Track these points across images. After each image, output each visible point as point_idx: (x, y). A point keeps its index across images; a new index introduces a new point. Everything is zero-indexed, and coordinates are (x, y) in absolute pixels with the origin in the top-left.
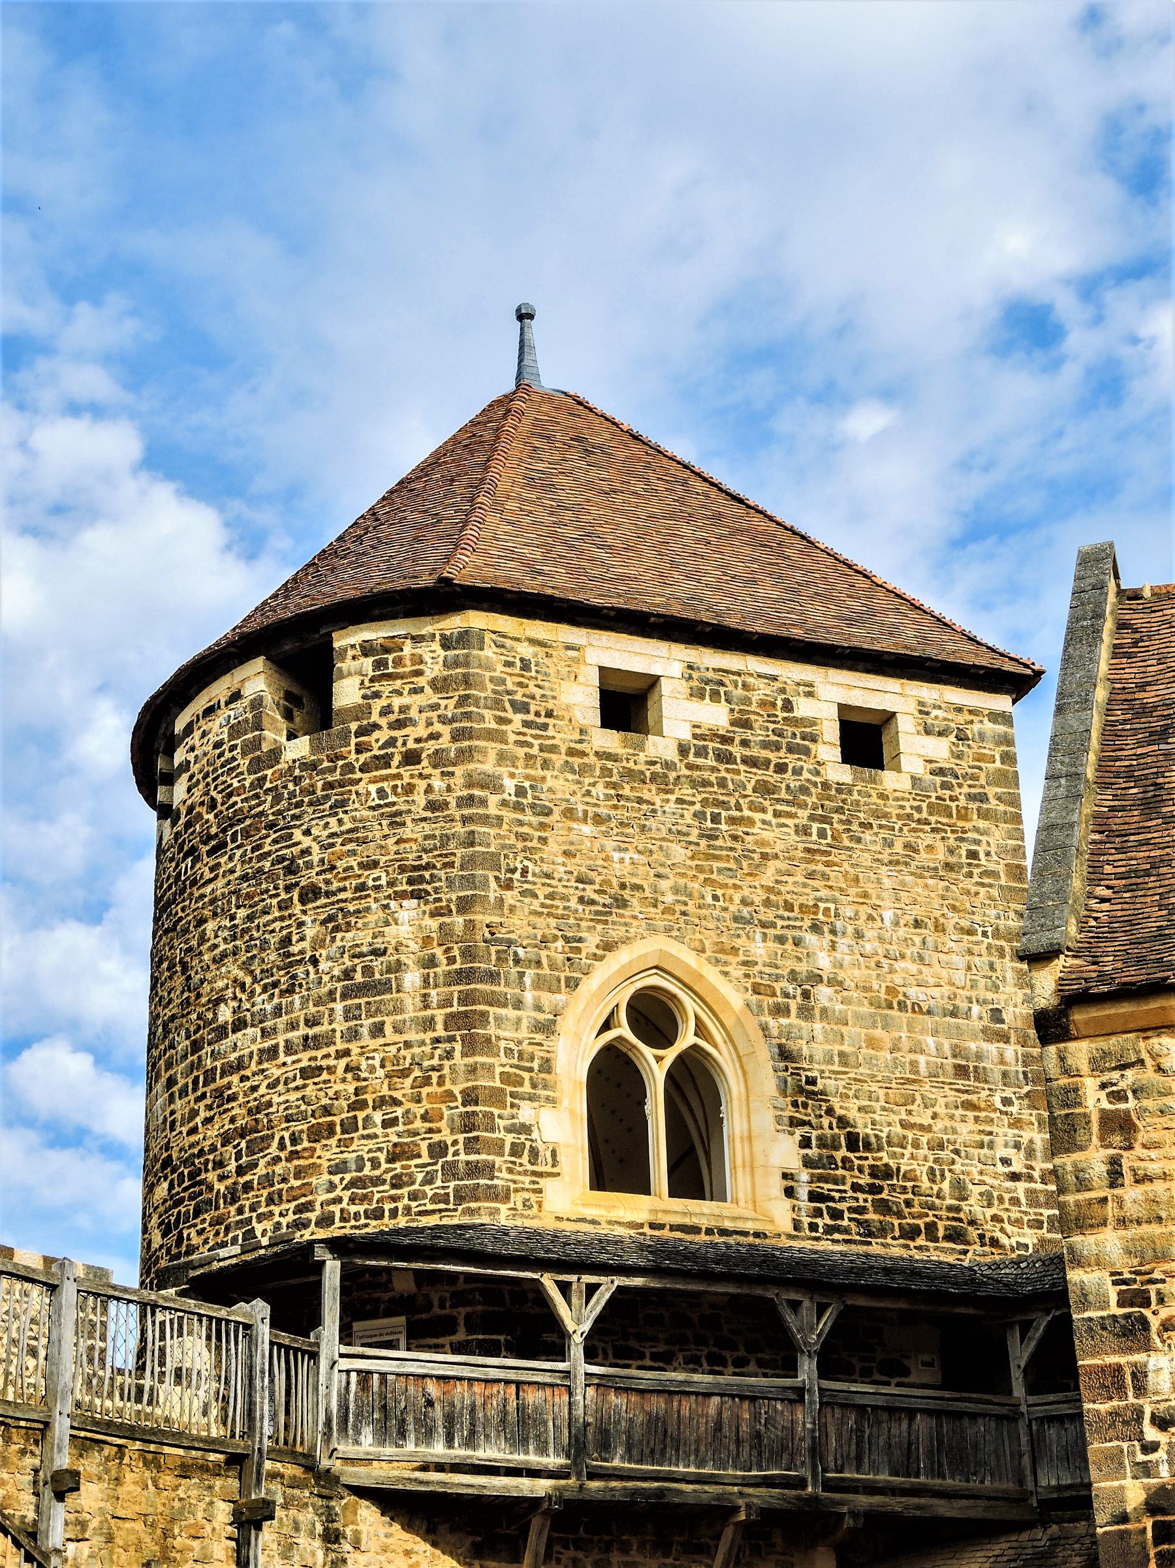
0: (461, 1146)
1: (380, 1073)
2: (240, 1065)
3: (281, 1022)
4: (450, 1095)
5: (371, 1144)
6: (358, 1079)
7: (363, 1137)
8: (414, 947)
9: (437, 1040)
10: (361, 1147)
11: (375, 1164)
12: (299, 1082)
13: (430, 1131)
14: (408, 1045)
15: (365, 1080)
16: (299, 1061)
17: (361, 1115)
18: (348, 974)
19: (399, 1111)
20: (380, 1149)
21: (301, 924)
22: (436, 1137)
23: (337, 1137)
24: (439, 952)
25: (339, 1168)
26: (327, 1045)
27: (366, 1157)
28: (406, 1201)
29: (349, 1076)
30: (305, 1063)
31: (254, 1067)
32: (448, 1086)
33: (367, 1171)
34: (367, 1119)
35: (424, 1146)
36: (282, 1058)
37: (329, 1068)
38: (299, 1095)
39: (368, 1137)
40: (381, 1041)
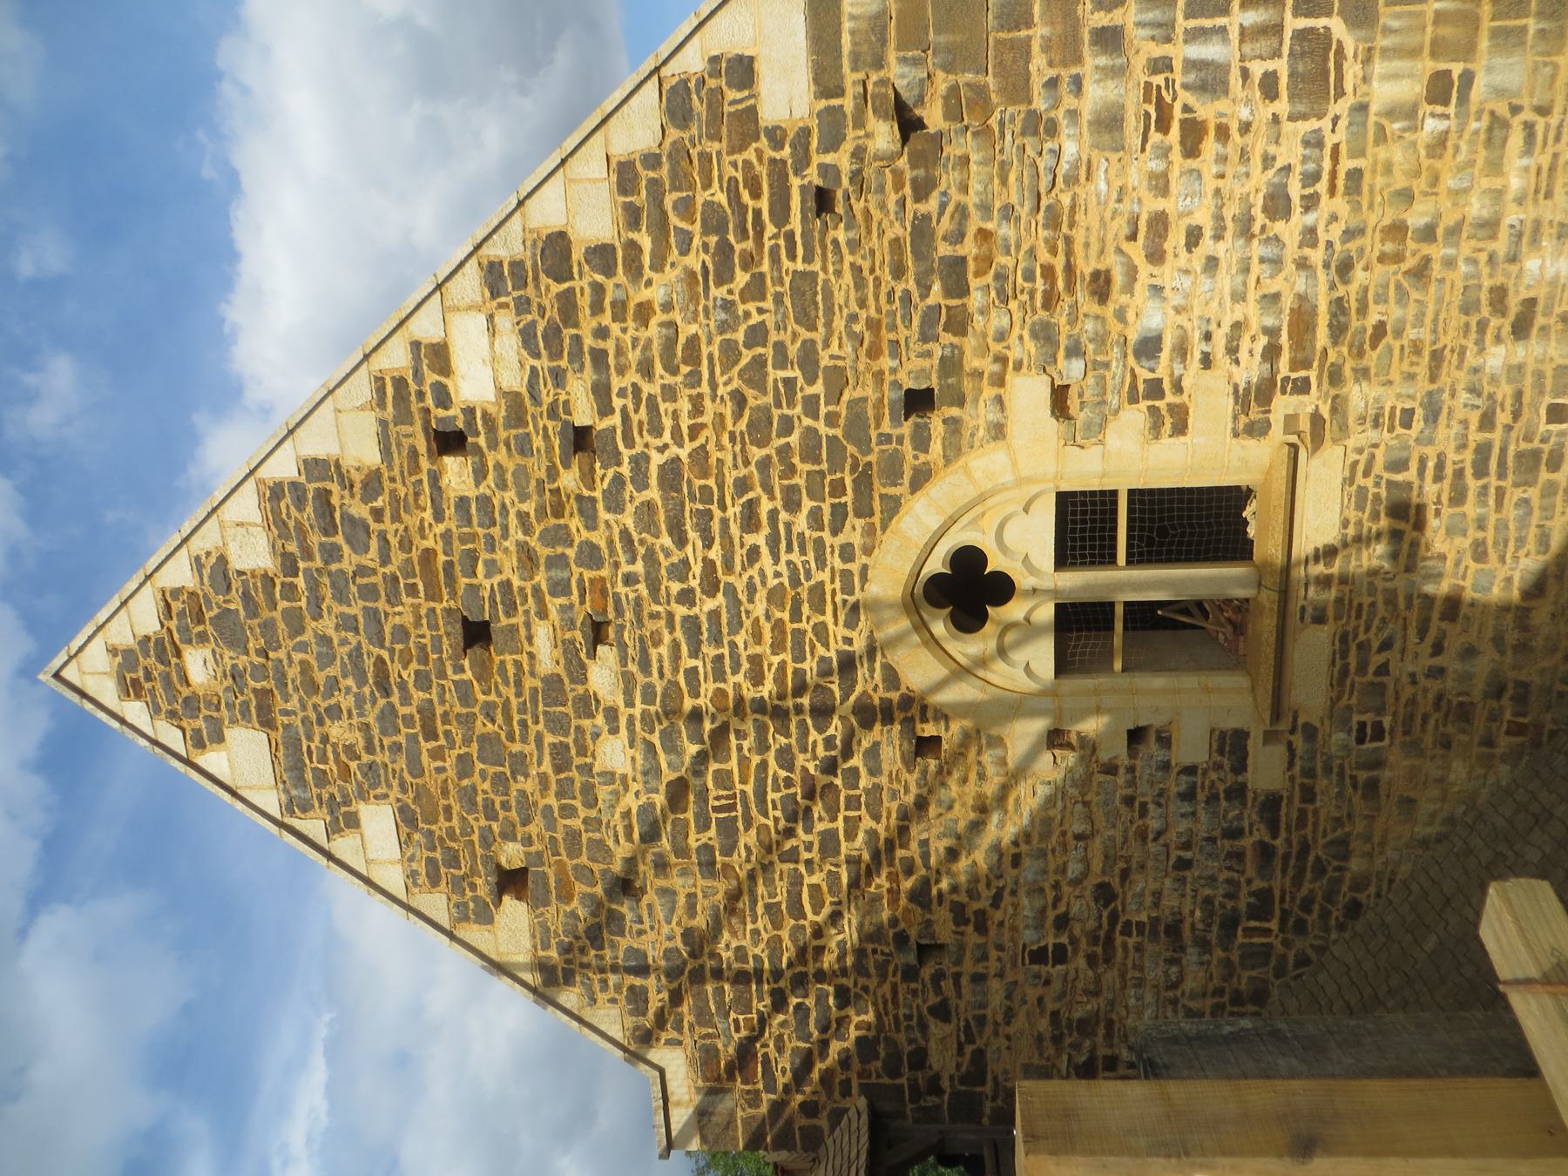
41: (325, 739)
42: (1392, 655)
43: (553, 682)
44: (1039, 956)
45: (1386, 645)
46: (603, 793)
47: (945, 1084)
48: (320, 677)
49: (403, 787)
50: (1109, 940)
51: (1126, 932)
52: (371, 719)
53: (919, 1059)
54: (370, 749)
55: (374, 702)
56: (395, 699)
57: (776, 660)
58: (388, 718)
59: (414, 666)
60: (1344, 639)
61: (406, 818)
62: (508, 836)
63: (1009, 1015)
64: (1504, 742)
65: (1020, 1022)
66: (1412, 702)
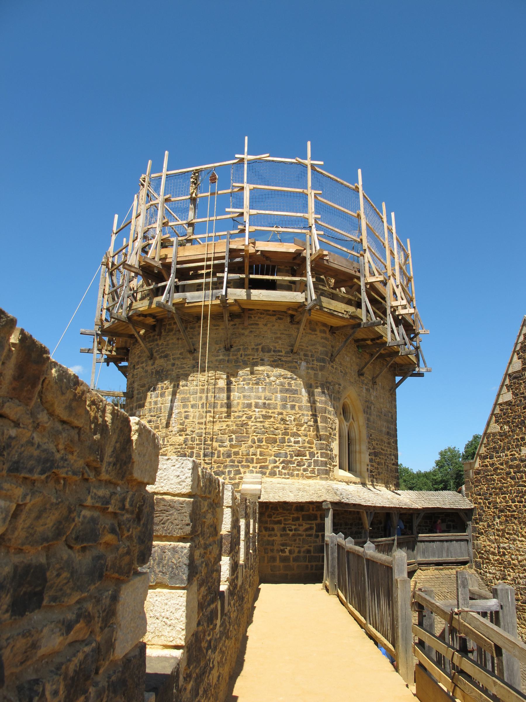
0: (319, 454)
3: (253, 394)
5: (290, 449)
7: (287, 446)
11: (292, 457)
12: (261, 420)
13: (310, 447)
14: (303, 415)
15: (288, 425)
16: (262, 411)
17: (287, 437)
18: (282, 384)
19: (300, 439)
22: (312, 450)
25: (277, 455)
26: (275, 408)
27: (288, 453)
28: (302, 472)
29: (282, 422)
30: (264, 413)
34: (289, 439)
36: (253, 408)
37: (274, 417)
39: (289, 446)
40: (294, 411)
53: (481, 520)
62: (510, 428)
65: (489, 543)
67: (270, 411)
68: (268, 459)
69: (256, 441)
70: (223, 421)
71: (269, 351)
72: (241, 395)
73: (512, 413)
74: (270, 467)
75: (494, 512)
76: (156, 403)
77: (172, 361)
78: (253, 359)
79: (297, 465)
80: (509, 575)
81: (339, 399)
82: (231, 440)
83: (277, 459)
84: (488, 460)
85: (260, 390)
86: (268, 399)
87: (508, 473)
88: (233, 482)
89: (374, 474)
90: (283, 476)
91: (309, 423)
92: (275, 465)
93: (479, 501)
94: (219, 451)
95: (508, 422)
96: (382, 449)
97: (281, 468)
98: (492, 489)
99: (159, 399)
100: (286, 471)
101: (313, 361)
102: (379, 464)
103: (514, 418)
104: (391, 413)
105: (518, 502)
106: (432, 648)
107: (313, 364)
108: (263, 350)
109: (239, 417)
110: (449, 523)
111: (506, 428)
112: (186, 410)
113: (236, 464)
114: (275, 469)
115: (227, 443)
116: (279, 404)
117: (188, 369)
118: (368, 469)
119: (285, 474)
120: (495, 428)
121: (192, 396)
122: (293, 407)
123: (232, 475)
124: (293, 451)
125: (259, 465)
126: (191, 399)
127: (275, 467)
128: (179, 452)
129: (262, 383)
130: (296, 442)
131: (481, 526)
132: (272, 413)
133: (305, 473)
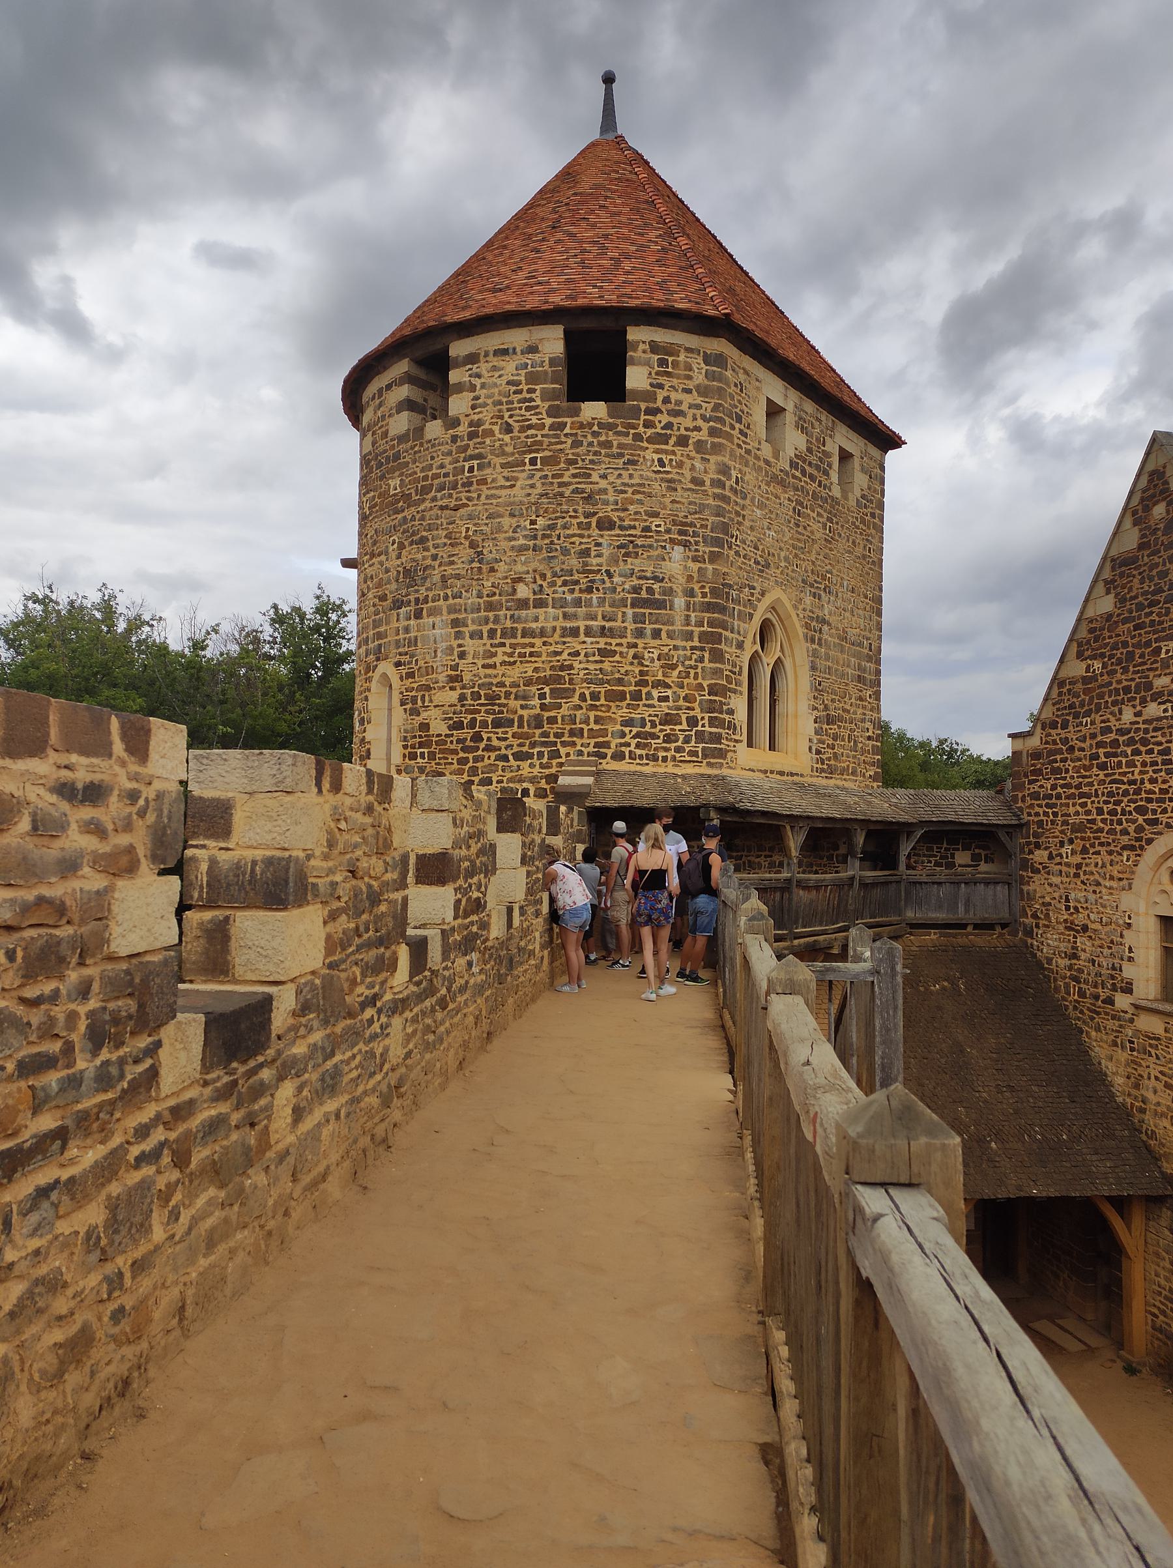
0: (706, 721)
1: (657, 663)
2: (542, 633)
3: (581, 611)
4: (700, 687)
5: (651, 711)
6: (642, 665)
7: (645, 705)
8: (682, 580)
9: (692, 648)
10: (642, 712)
11: (654, 725)
12: (597, 658)
13: (688, 708)
14: (676, 648)
17: (644, 690)
18: (636, 590)
19: (669, 693)
20: (657, 716)
21: (598, 545)
22: (692, 713)
23: (628, 701)
24: (696, 587)
26: (621, 637)
29: (636, 661)
30: (602, 646)
31: (556, 637)
32: (700, 680)
33: (648, 728)
35: (684, 717)
36: (582, 637)
37: (621, 653)
38: (598, 666)
40: (658, 642)
41: (1134, 576)
42: (1153, 1059)
43: (1149, 686)
44: (1067, 900)
45: (1158, 1058)
46: (1116, 709)
47: (1031, 856)
48: (1154, 572)
49: (1119, 615)
50: (1073, 929)
51: (1075, 937)
52: (1140, 599)
53: (1038, 846)
54: (1132, 598)
55: (1146, 599)
56: (1147, 610)
57: (1157, 790)
58: (1140, 607)
59: (1157, 619)
60: (1159, 1039)
61: (1109, 616)
62: (1104, 666)
63: (1050, 885)
64: (1129, 1100)
65: (1049, 889)
66: (1141, 1066)
67: (614, 642)
68: (610, 730)
69: (588, 697)
70: (528, 662)
71: (611, 525)
72: (559, 612)
73: (1110, 637)
74: (613, 745)
75: (1062, 832)
76: (407, 630)
77: (433, 551)
78: (581, 543)
79: (664, 741)
80: (1084, 951)
81: (751, 616)
82: (542, 696)
83: (627, 730)
84: (1059, 731)
85: (595, 601)
86: (610, 620)
87: (1095, 757)
88: (547, 771)
89: (824, 757)
90: (638, 761)
91: (687, 663)
92: (623, 741)
93: (1037, 809)
94: (521, 717)
95: (1102, 655)
96: (844, 710)
97: (633, 745)
98: (1062, 786)
99: (412, 622)
100: (644, 752)
101: (697, 543)
102: (835, 738)
103: (1112, 649)
104: (868, 639)
105: (1108, 813)
106: (329, 937)
107: (697, 550)
108: (600, 526)
109: (556, 653)
110: (977, 851)
111: (1097, 665)
112: (460, 642)
113: (552, 739)
114: (623, 749)
115: (536, 702)
116: (629, 628)
117: (461, 566)
118: (810, 748)
119: (641, 757)
120: (1077, 669)
121: (470, 616)
122: (656, 634)
123: (545, 760)
124: (657, 716)
125: (592, 742)
126: (470, 622)
127: (622, 745)
128: (451, 718)
129: (597, 589)
130: (661, 699)
131: (1040, 856)
132: (617, 645)
133: (678, 755)
